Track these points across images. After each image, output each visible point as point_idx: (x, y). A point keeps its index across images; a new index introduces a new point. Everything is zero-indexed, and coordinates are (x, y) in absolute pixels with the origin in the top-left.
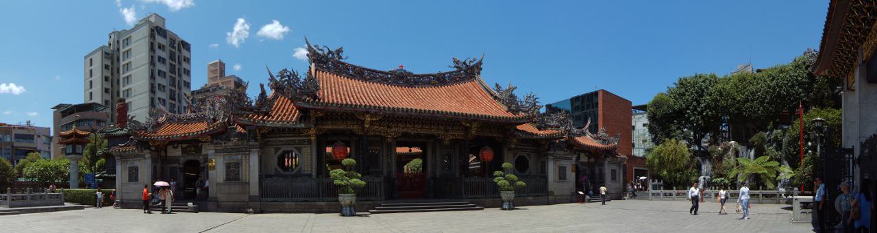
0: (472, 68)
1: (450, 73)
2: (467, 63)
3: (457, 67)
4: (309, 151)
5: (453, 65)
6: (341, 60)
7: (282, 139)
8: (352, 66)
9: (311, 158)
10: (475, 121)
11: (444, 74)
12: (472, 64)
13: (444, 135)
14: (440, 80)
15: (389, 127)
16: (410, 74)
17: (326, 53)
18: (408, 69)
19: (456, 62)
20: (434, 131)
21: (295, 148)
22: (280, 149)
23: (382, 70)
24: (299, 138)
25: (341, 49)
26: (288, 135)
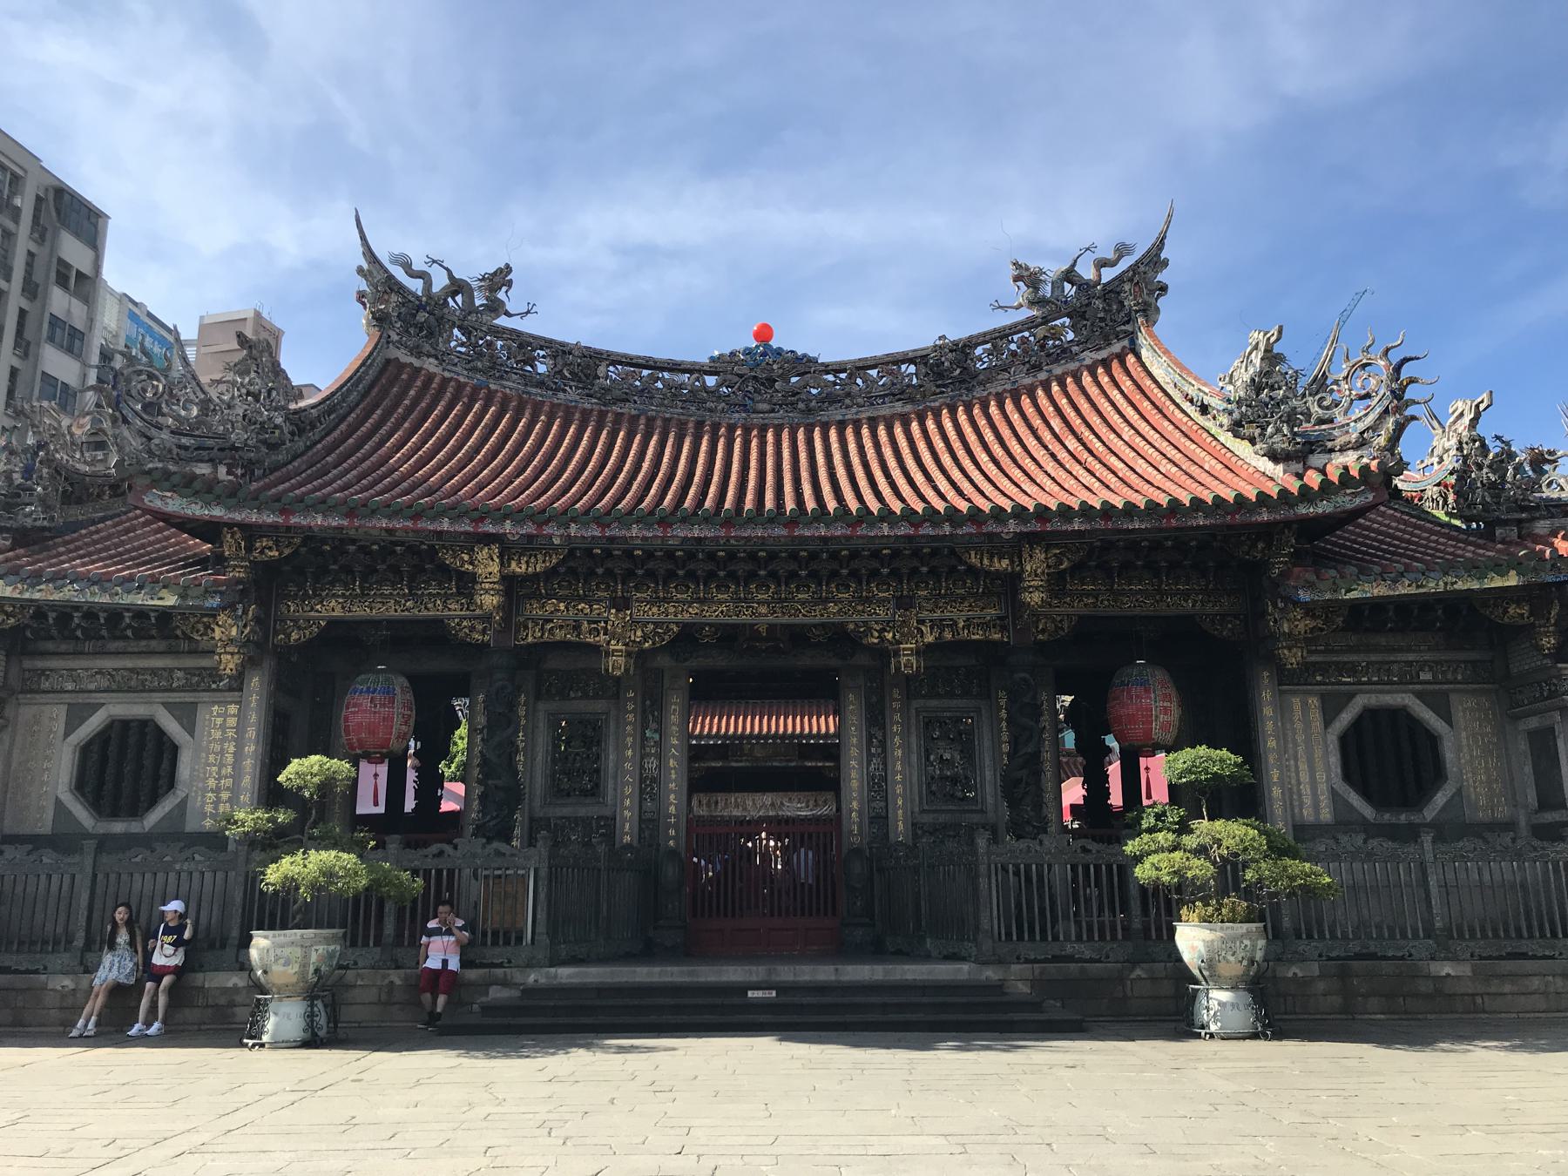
0: (1112, 291)
1: (1003, 335)
2: (1087, 272)
4: (232, 722)
6: (502, 321)
8: (547, 344)
9: (238, 755)
10: (1033, 539)
11: (963, 349)
12: (1108, 275)
13: (888, 625)
14: (947, 377)
15: (622, 604)
16: (804, 365)
17: (436, 289)
20: (835, 609)
22: (95, 707)
23: (678, 357)
24: (190, 662)
25: (508, 269)
26: (133, 646)
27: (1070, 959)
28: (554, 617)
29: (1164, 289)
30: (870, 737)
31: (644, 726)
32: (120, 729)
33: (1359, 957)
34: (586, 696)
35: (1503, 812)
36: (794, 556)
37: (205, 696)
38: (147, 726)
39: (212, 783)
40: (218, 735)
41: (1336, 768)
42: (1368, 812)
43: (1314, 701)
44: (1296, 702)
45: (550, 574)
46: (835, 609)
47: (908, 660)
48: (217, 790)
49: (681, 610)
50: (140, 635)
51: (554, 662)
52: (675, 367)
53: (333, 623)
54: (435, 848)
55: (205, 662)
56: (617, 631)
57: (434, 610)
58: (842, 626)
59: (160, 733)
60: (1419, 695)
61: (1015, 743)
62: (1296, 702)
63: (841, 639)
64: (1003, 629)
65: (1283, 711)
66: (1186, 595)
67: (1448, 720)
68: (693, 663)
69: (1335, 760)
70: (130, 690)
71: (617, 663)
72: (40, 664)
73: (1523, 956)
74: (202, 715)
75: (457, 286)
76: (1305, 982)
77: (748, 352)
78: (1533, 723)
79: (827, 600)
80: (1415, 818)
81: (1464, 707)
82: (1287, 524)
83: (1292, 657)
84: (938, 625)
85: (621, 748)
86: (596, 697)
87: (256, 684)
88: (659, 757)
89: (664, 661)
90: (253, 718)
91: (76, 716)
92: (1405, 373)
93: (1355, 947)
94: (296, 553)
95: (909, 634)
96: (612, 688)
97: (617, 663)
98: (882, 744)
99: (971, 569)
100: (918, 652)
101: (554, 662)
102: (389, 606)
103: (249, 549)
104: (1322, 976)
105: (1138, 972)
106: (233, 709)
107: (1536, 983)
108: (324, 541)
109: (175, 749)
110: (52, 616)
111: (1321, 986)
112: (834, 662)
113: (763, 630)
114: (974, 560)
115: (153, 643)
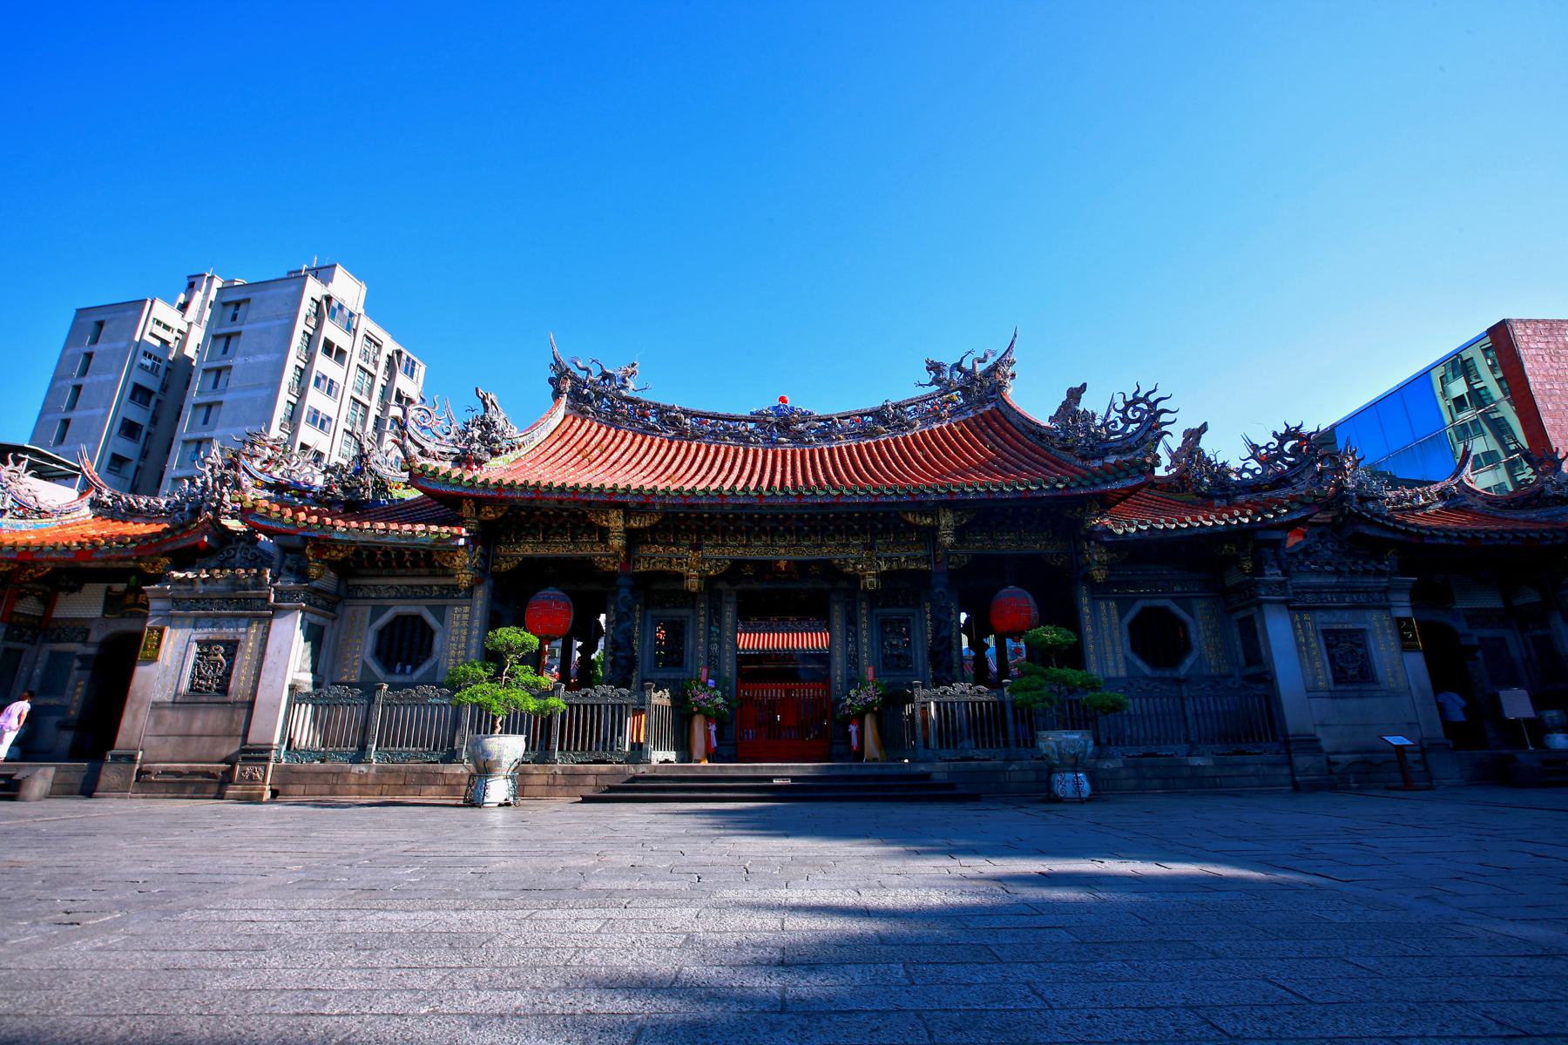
1: (925, 400)
2: (967, 365)
3: (936, 381)
4: (466, 617)
5: (927, 378)
7: (396, 582)
8: (657, 406)
9: (468, 637)
12: (980, 368)
15: (697, 547)
16: (805, 417)
18: (800, 402)
19: (934, 367)
20: (828, 551)
21: (428, 607)
24: (443, 581)
27: (971, 759)
28: (655, 557)
29: (1013, 375)
30: (848, 631)
31: (711, 625)
32: (400, 620)
33: (1145, 755)
34: (675, 607)
35: (1225, 670)
36: (800, 517)
37: (450, 602)
38: (417, 619)
39: (453, 653)
40: (457, 624)
41: (1127, 645)
42: (1147, 670)
43: (1112, 604)
44: (1103, 605)
45: (653, 529)
46: (828, 551)
47: (870, 581)
48: (456, 658)
49: (735, 551)
50: (415, 565)
51: (657, 586)
52: (731, 419)
53: (528, 561)
54: (584, 691)
55: (450, 581)
56: (693, 564)
57: (585, 551)
58: (829, 561)
59: (424, 623)
60: (1174, 599)
61: (936, 632)
62: (1103, 605)
63: (829, 569)
64: (928, 562)
65: (1095, 610)
66: (1036, 542)
67: (1192, 616)
68: (739, 587)
69: (1126, 638)
70: (408, 597)
71: (693, 584)
72: (357, 582)
73: (1243, 753)
74: (448, 611)
75: (605, 376)
76: (1115, 771)
77: (775, 408)
78: (1241, 614)
79: (820, 546)
80: (1176, 674)
81: (1199, 606)
82: (1094, 495)
83: (1099, 575)
84: (888, 560)
85: (696, 637)
86: (681, 607)
87: (481, 594)
88: (719, 643)
89: (722, 586)
90: (478, 613)
91: (377, 612)
92: (1160, 406)
93: (1143, 749)
94: (505, 516)
95: (867, 565)
96: (689, 599)
97: (693, 584)
98: (855, 635)
99: (908, 524)
100: (877, 576)
101: (657, 586)
102: (560, 549)
103: (478, 512)
104: (1126, 767)
105: (1013, 767)
106: (466, 609)
107: (1251, 769)
108: (521, 509)
109: (432, 633)
110: (365, 554)
111: (1124, 773)
112: (826, 586)
113: (782, 565)
114: (910, 518)
115: (422, 571)
